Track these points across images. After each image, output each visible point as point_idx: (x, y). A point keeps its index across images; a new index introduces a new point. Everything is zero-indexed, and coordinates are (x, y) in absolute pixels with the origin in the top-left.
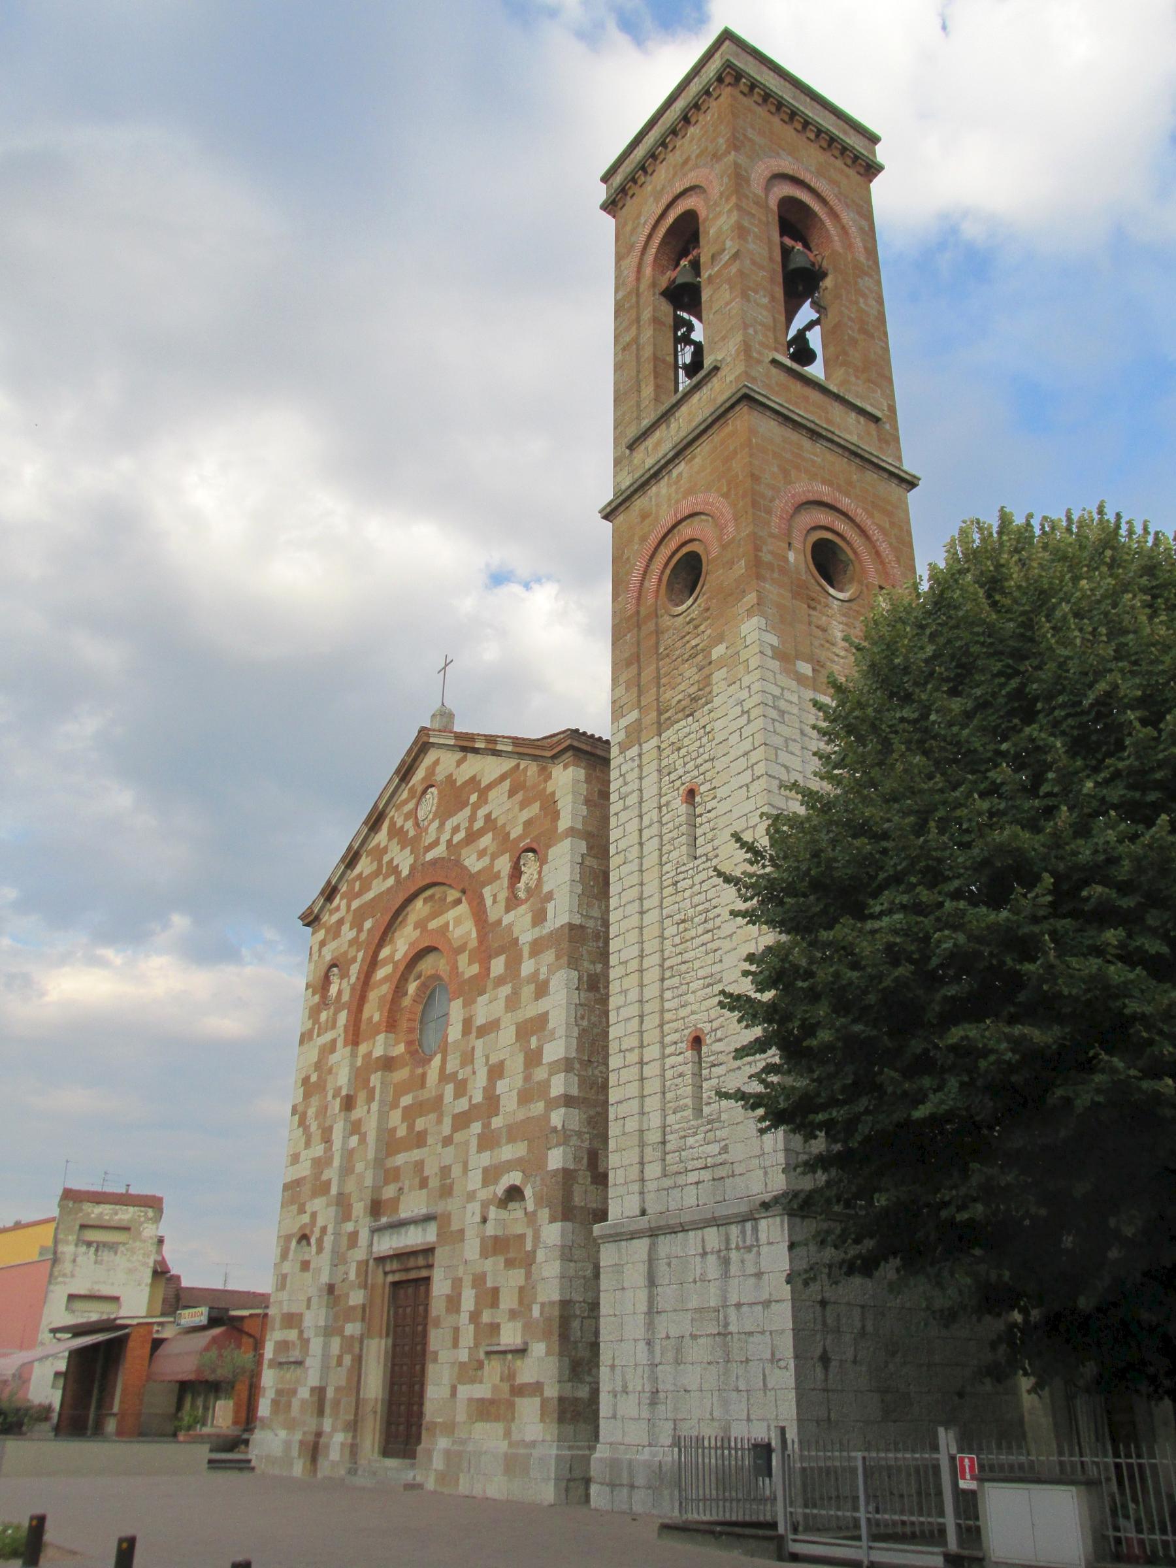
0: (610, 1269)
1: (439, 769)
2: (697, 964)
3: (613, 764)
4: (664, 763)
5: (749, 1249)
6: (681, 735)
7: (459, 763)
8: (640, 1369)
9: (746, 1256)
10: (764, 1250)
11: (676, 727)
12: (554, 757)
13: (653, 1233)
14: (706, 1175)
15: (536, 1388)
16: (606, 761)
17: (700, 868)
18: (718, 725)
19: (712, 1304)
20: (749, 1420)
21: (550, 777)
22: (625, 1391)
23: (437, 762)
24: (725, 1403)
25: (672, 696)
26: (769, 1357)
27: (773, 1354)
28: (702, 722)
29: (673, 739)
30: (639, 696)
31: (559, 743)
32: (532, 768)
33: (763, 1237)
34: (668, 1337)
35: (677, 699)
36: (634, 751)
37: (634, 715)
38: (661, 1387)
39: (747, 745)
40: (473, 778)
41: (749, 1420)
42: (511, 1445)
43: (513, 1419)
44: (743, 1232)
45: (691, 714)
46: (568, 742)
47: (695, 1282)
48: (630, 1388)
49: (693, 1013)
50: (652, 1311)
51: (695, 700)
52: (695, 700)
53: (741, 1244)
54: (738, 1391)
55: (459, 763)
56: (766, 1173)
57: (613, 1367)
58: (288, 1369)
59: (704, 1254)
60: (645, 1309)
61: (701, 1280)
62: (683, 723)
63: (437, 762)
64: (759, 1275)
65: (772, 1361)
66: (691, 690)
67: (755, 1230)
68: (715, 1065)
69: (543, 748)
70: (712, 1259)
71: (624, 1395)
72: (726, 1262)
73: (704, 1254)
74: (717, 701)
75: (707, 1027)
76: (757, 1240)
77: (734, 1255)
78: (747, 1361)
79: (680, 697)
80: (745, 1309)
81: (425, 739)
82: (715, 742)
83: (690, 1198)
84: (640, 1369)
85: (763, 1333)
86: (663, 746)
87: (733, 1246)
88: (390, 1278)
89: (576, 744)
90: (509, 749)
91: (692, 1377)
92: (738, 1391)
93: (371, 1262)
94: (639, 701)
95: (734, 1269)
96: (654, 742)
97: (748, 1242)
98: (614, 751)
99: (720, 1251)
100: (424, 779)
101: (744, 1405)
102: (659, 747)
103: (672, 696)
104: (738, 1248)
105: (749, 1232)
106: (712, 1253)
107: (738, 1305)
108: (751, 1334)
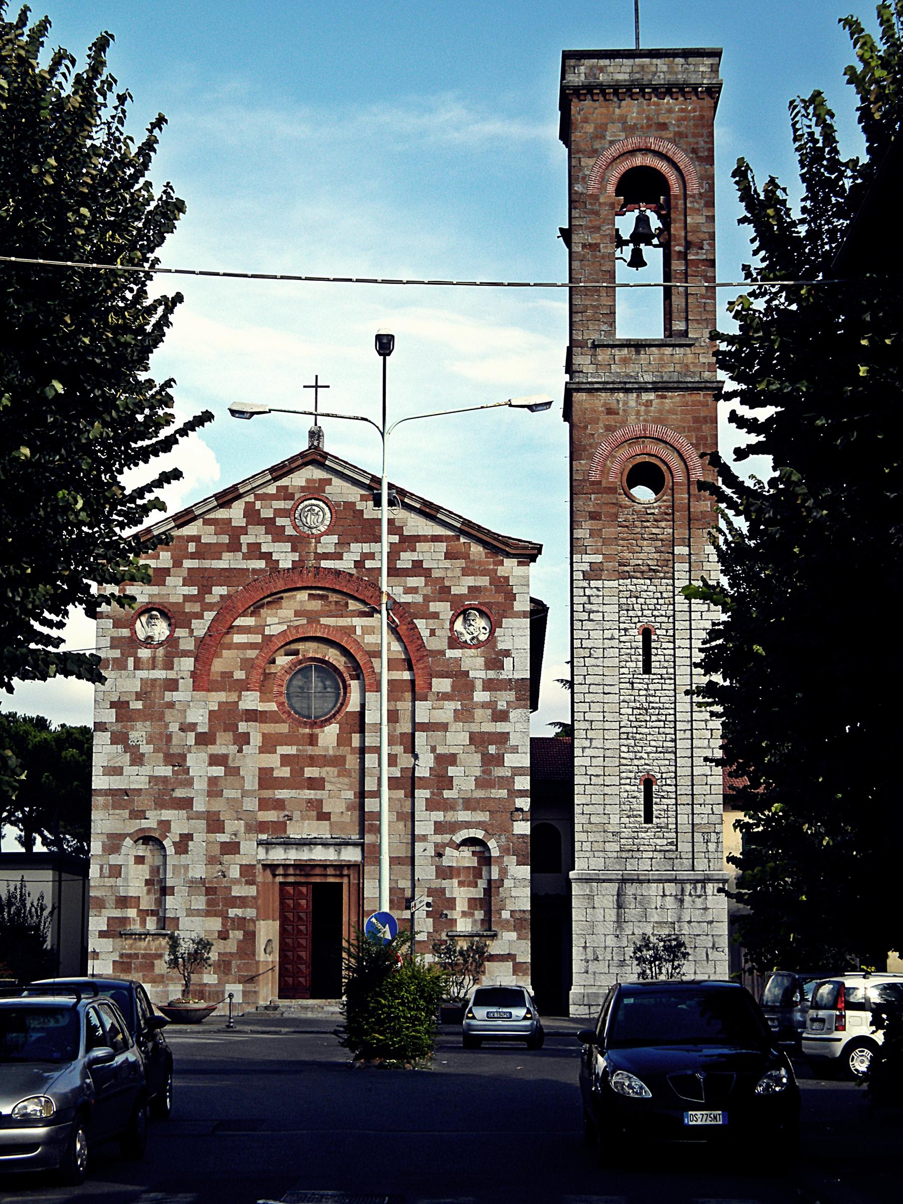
5: (699, 896)
8: (609, 950)
13: (624, 881)
14: (661, 855)
15: (510, 957)
19: (670, 920)
22: (596, 959)
26: (711, 945)
27: (714, 945)
31: (526, 548)
34: (633, 934)
44: (695, 888)
45: (650, 579)
48: (600, 958)
49: (646, 764)
50: (620, 922)
56: (709, 861)
57: (585, 947)
58: (126, 939)
59: (664, 895)
60: (614, 918)
64: (706, 909)
65: (713, 948)
67: (704, 888)
72: (682, 901)
73: (664, 895)
76: (705, 892)
77: (687, 898)
78: (695, 947)
83: (645, 865)
84: (609, 950)
85: (707, 935)
88: (280, 879)
95: (686, 905)
97: (698, 893)
101: (692, 967)
104: (690, 895)
106: (671, 895)
107: (689, 922)
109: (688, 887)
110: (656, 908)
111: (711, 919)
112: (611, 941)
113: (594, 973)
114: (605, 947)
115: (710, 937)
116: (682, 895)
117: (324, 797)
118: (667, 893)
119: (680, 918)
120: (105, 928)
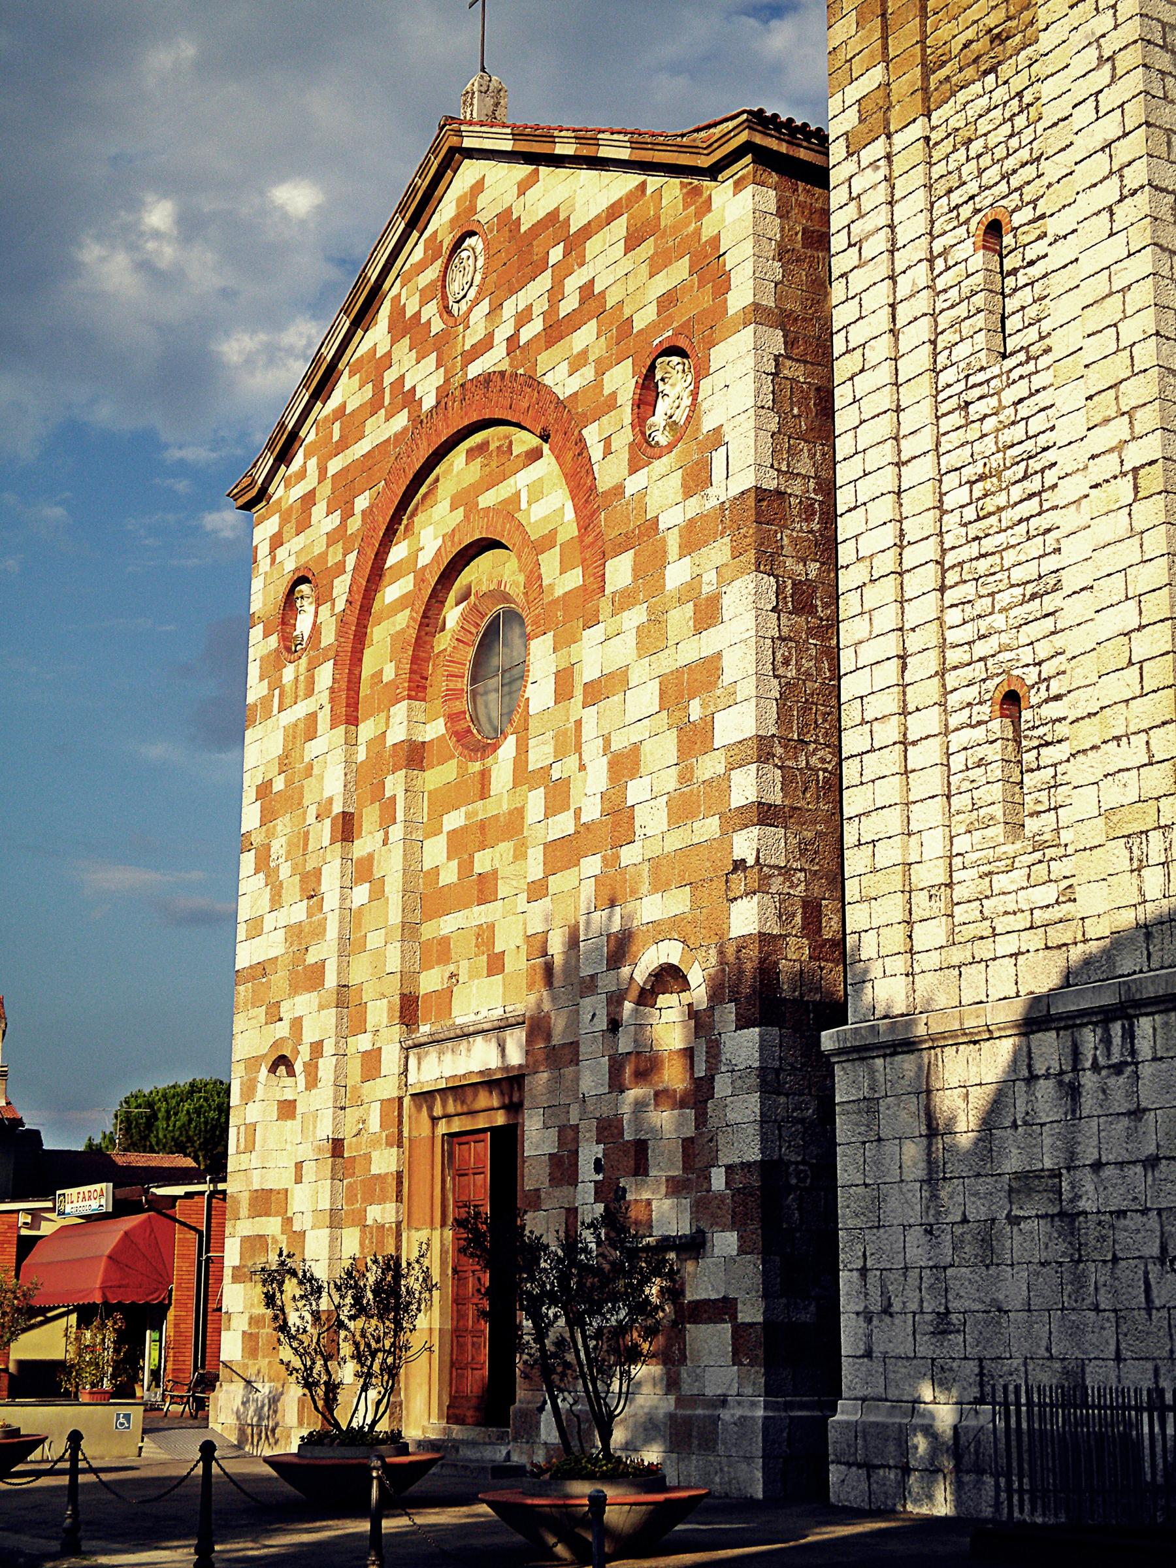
0: (854, 1107)
1: (482, 201)
2: (1010, 557)
3: (835, 177)
4: (937, 171)
5: (1118, 1069)
6: (972, 111)
7: (523, 188)
8: (913, 1274)
9: (1112, 1081)
10: (1146, 1070)
11: (962, 96)
12: (713, 172)
14: (1033, 940)
15: (723, 1309)
16: (819, 177)
17: (1015, 375)
18: (1048, 89)
19: (1048, 1164)
20: (1118, 1358)
21: (708, 205)
22: (887, 1311)
23: (478, 187)
24: (1076, 1332)
25: (949, 34)
26: (1155, 1251)
28: (1017, 84)
29: (956, 122)
30: (885, 38)
31: (725, 138)
32: (672, 188)
33: (1144, 1048)
34: (965, 1221)
35: (962, 39)
36: (878, 148)
37: (877, 75)
38: (954, 1305)
39: (1110, 127)
40: (553, 216)
41: (1118, 1358)
42: (679, 1402)
43: (683, 1360)
44: (1107, 1041)
45: (993, 69)
46: (744, 137)
47: (1015, 1126)
48: (897, 1307)
51: (999, 39)
52: (999, 39)
53: (1102, 1061)
54: (1097, 1309)
55: (523, 188)
57: (863, 1271)
61: (1025, 1123)
62: (976, 88)
63: (478, 187)
64: (1137, 1113)
65: (1162, 1258)
66: (991, 21)
67: (1129, 1035)
68: (1047, 744)
69: (693, 150)
70: (1045, 1088)
71: (887, 1319)
72: (1073, 1092)
73: (1032, 1079)
74: (1046, 41)
75: (1031, 675)
76: (1133, 1052)
77: (1088, 1080)
78: (1115, 1259)
79: (970, 34)
80: (1108, 1172)
81: (454, 141)
82: (1040, 126)
85: (1145, 1212)
86: (935, 136)
87: (1088, 1064)
88: (442, 1128)
89: (758, 139)
90: (624, 154)
91: (1013, 1288)
92: (1097, 1309)
93: (407, 1101)
94: (885, 47)
95: (1088, 1104)
96: (917, 129)
97: (1115, 1060)
98: (837, 151)
99: (1062, 1072)
100: (452, 221)
101: (1110, 1333)
102: (927, 139)
103: (949, 34)
105: (1117, 1041)
106: (1047, 1076)
107: (1097, 1166)
108: (1121, 1214)
109: (1089, 1038)
110: (1015, 1126)
111: (1151, 1149)
112: (917, 1251)
113: (885, 1356)
114: (906, 1268)
115: (1153, 1221)
116: (1075, 1069)
117: (498, 916)
118: (1040, 1070)
119: (1072, 1155)
120: (237, 1264)
